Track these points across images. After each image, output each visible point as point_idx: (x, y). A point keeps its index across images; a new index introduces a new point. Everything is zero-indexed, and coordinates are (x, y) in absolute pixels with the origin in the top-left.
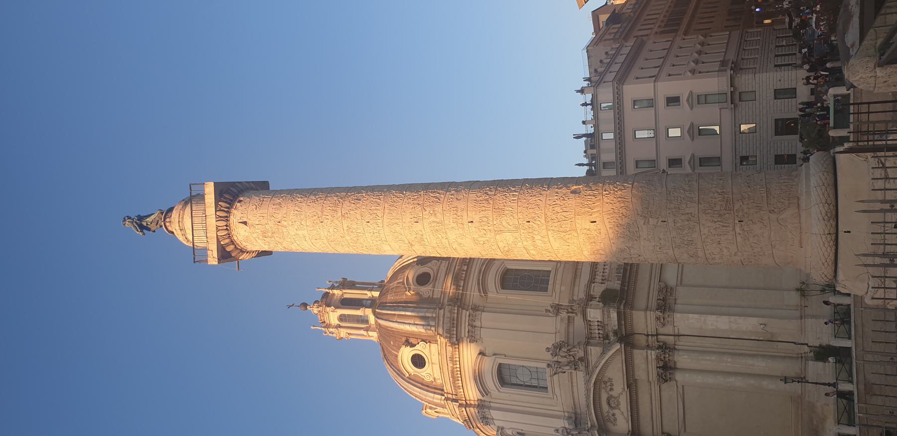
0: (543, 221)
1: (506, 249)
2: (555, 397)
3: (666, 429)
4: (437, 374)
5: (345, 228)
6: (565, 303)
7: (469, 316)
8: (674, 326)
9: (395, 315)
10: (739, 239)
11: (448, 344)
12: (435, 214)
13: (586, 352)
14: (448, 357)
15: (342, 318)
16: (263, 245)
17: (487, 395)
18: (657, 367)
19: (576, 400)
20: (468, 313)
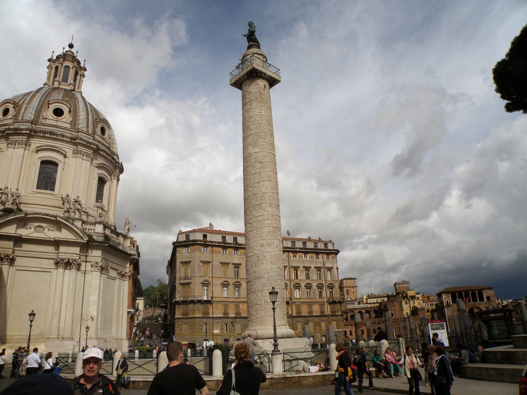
3: (18, 259)
7: (90, 154)
9: (87, 108)
14: (64, 133)
16: (254, 90)
18: (69, 259)
20: (91, 153)
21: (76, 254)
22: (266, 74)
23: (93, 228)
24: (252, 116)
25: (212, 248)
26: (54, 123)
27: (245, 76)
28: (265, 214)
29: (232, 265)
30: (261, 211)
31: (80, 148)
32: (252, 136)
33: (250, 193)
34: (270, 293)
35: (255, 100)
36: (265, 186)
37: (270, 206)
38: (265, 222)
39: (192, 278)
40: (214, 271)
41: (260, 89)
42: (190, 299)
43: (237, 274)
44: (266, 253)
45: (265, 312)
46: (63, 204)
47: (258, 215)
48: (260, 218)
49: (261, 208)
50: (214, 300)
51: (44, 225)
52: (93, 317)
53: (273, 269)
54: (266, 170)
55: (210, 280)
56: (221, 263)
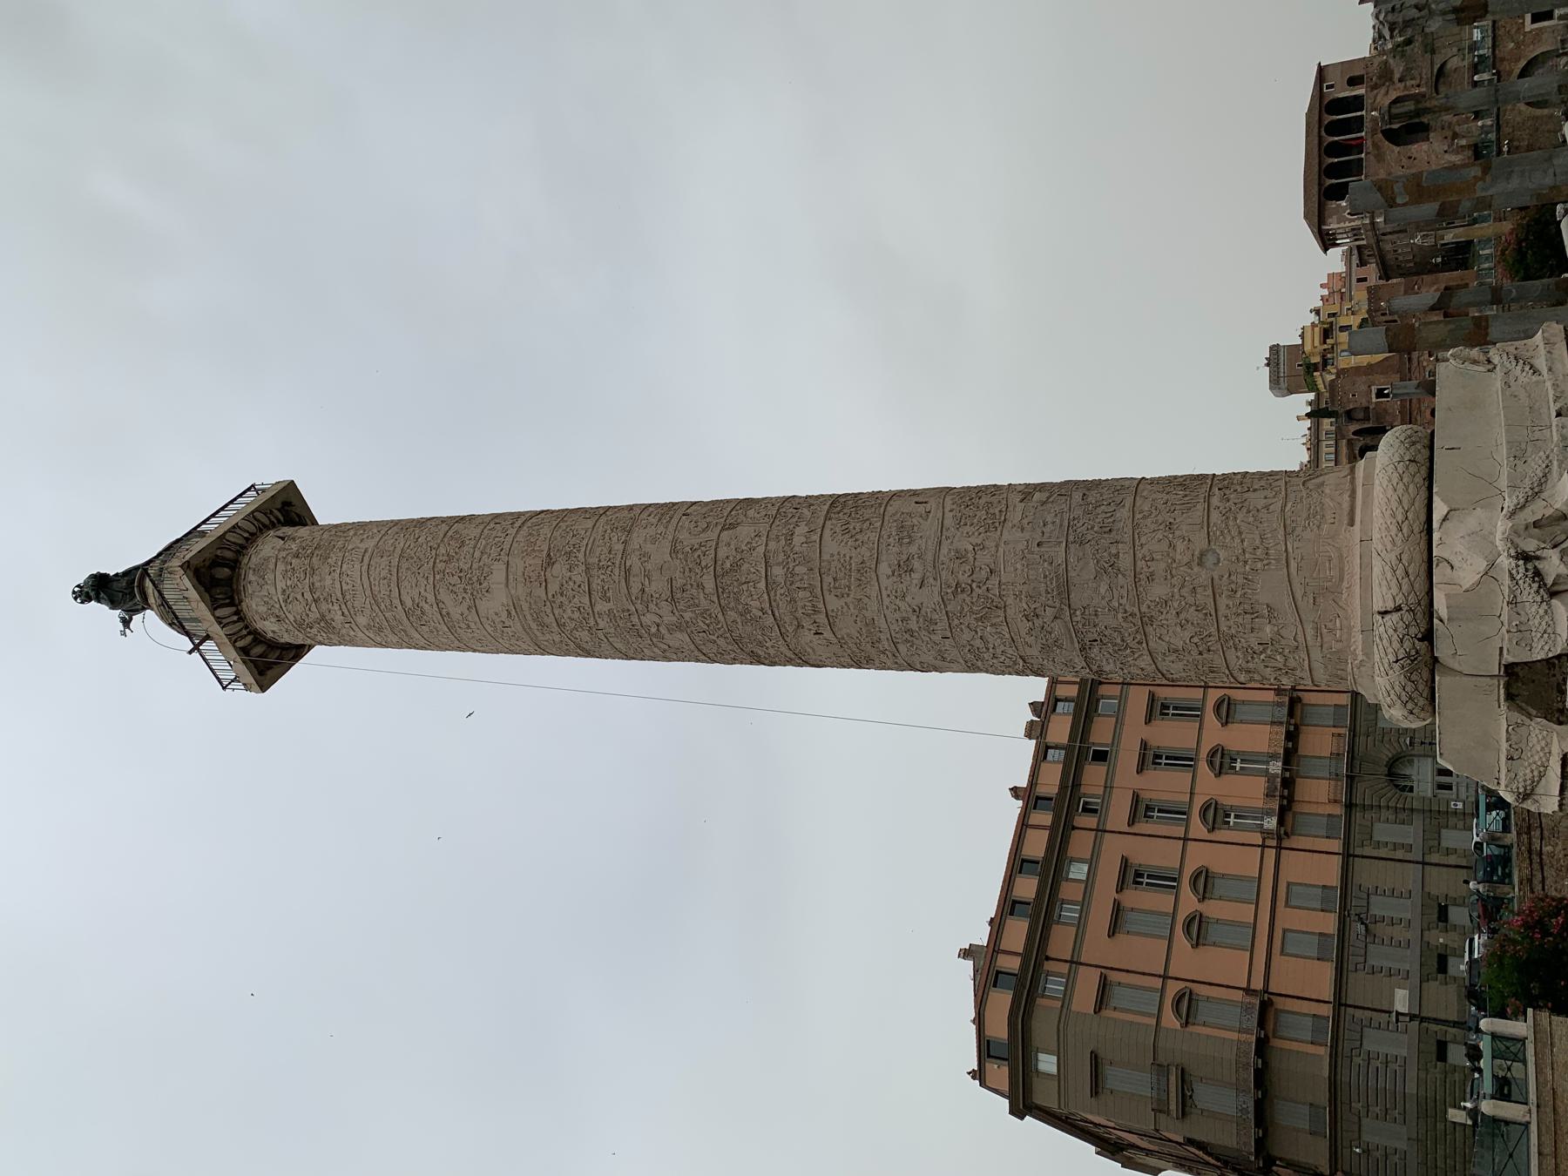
1: (728, 565)
16: (279, 577)
24: (368, 592)
28: (761, 549)
30: (746, 566)
32: (444, 596)
33: (669, 619)
35: (316, 578)
36: (649, 547)
38: (797, 549)
41: (283, 554)
43: (1165, 880)
44: (944, 551)
45: (1259, 565)
47: (762, 585)
48: (778, 571)
49: (736, 566)
50: (1258, 984)
53: (1030, 519)
54: (585, 542)
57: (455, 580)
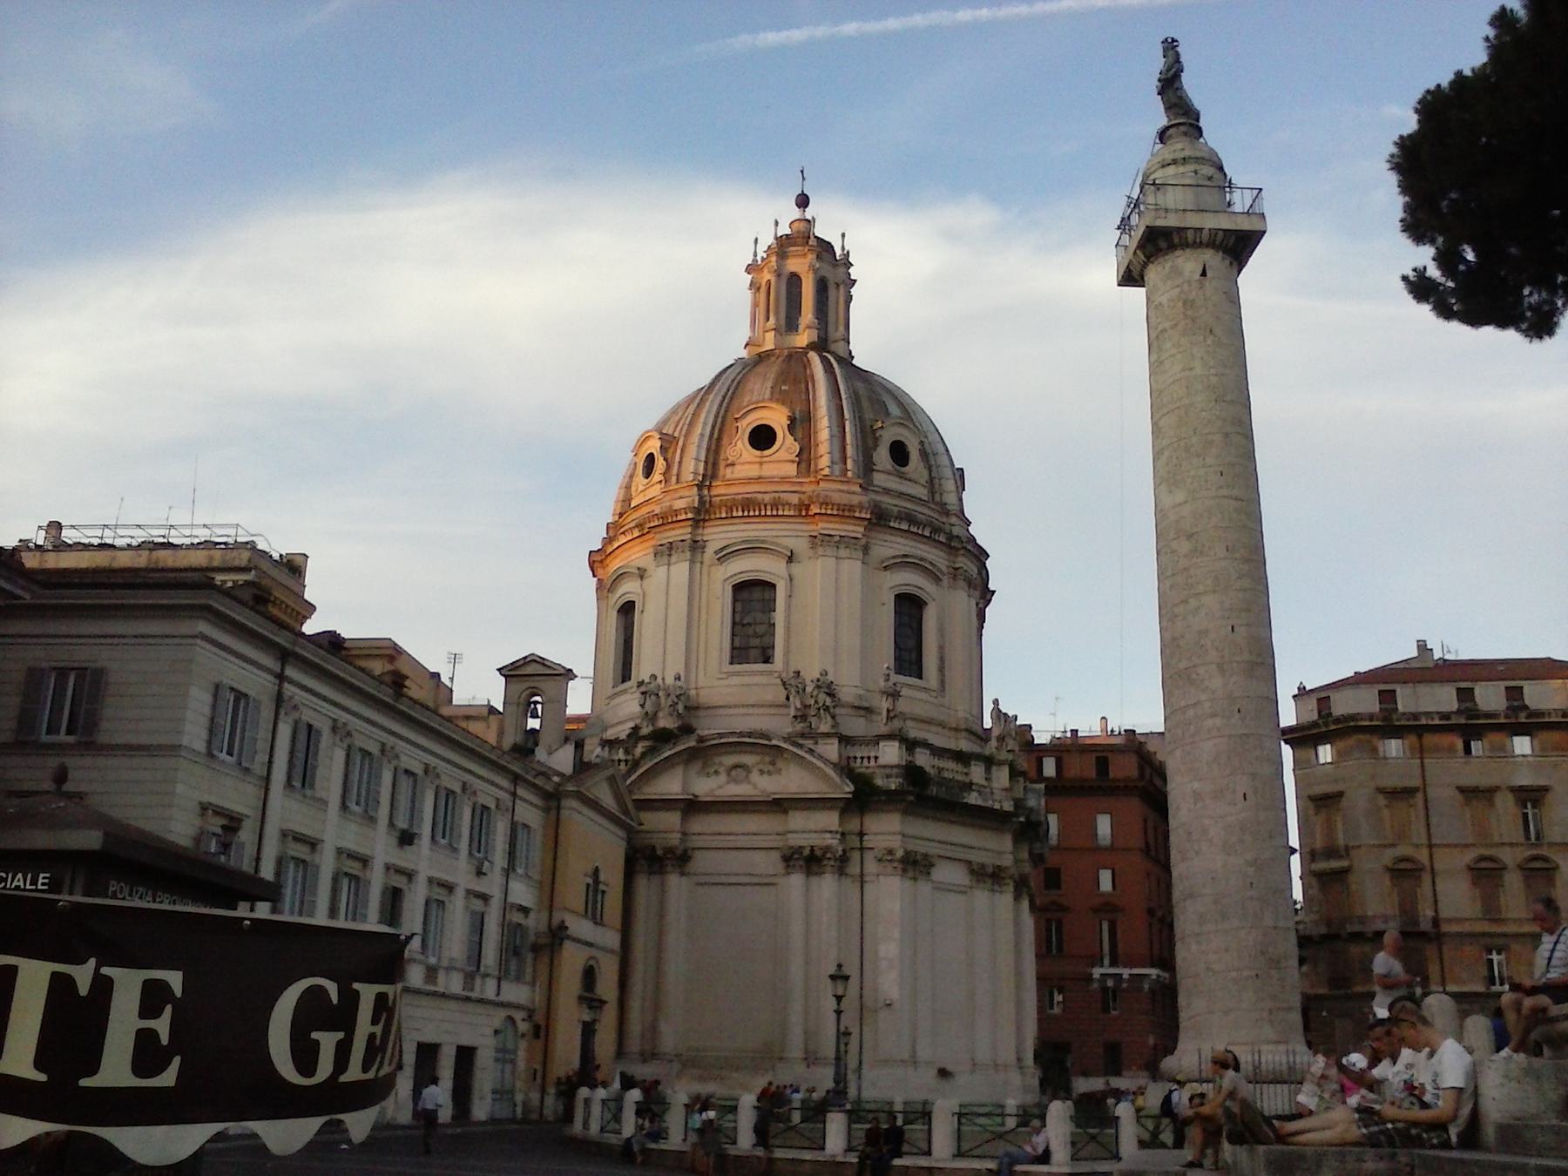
0: (1241, 732)
1: (1194, 676)
2: (723, 676)
3: (698, 855)
4: (741, 471)
5: (1210, 437)
6: (902, 705)
8: (878, 875)
10: (1234, 974)
11: (802, 496)
12: (1239, 578)
13: (827, 735)
15: (794, 280)
17: (718, 559)
18: (812, 847)
19: (721, 711)
21: (831, 832)
22: (1201, 229)
23: (872, 754)
25: (1420, 737)
26: (753, 471)
27: (1138, 252)
29: (1510, 796)
31: (823, 527)
34: (833, 977)
37: (1221, 669)
39: (1353, 853)
40: (1434, 820)
42: (1349, 928)
46: (788, 698)
47: (1183, 703)
48: (1191, 713)
50: (1445, 928)
51: (748, 759)
52: (888, 1002)
55: (1423, 856)
56: (1461, 790)
57: (1175, 461)
